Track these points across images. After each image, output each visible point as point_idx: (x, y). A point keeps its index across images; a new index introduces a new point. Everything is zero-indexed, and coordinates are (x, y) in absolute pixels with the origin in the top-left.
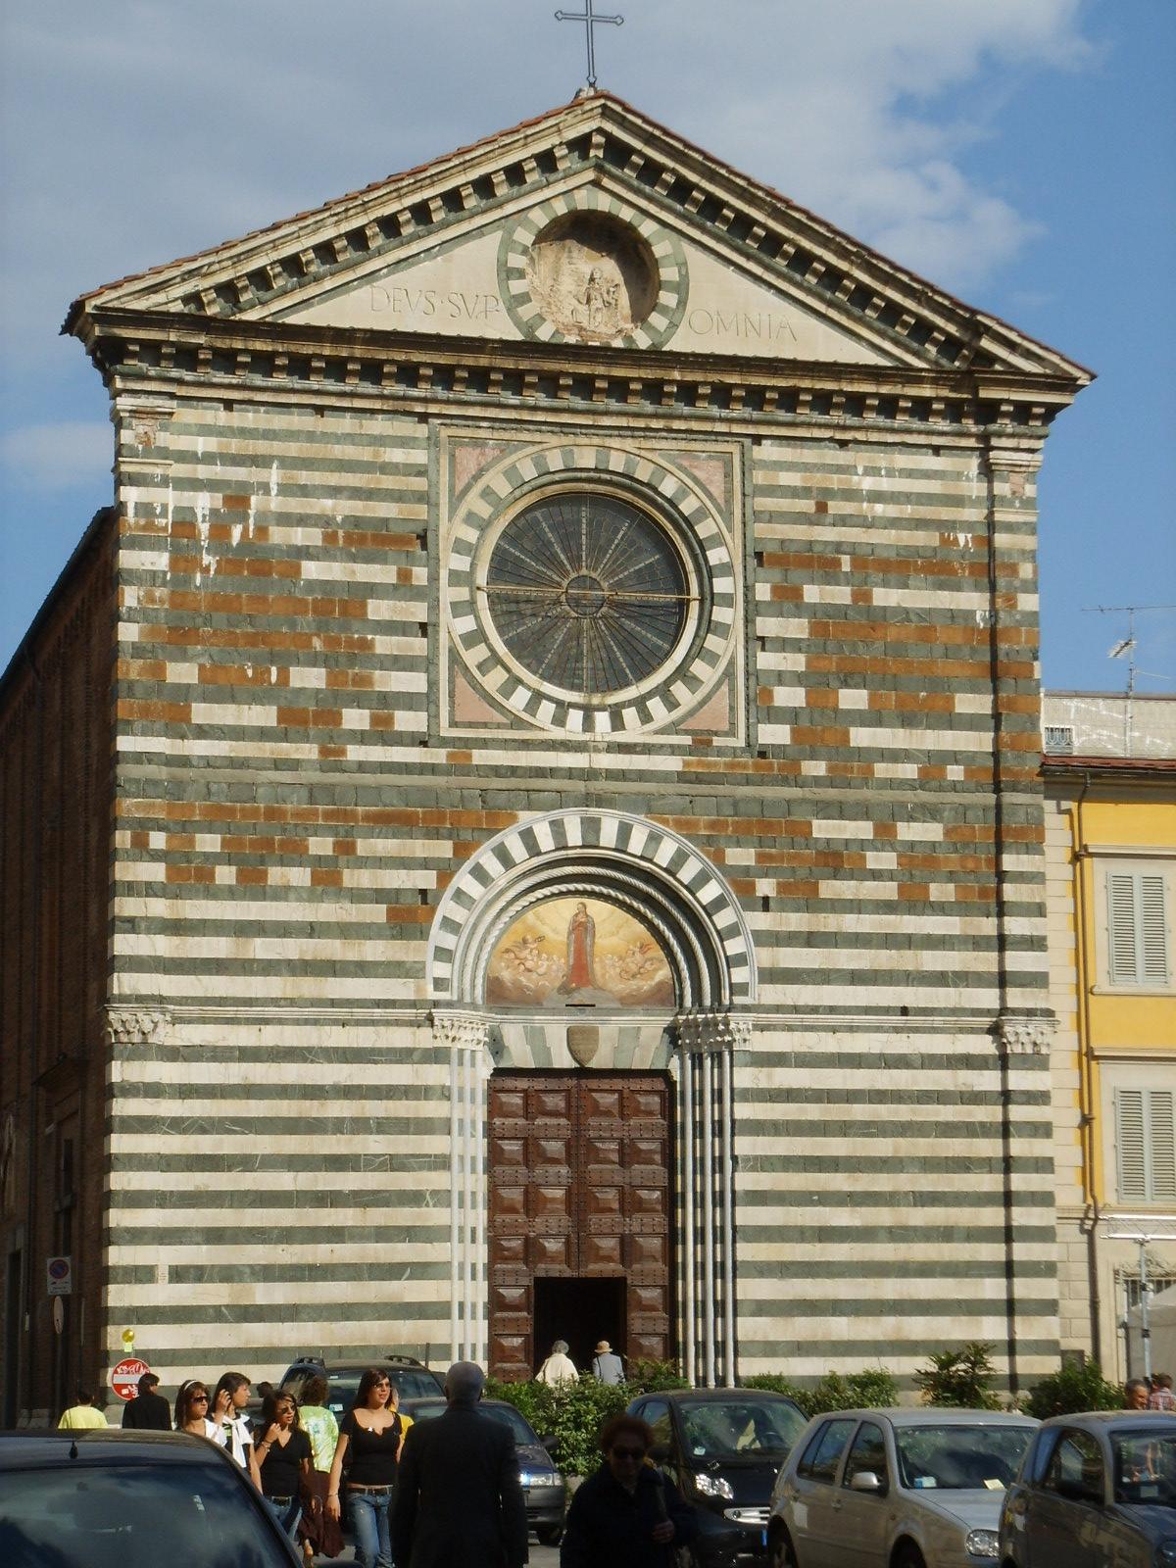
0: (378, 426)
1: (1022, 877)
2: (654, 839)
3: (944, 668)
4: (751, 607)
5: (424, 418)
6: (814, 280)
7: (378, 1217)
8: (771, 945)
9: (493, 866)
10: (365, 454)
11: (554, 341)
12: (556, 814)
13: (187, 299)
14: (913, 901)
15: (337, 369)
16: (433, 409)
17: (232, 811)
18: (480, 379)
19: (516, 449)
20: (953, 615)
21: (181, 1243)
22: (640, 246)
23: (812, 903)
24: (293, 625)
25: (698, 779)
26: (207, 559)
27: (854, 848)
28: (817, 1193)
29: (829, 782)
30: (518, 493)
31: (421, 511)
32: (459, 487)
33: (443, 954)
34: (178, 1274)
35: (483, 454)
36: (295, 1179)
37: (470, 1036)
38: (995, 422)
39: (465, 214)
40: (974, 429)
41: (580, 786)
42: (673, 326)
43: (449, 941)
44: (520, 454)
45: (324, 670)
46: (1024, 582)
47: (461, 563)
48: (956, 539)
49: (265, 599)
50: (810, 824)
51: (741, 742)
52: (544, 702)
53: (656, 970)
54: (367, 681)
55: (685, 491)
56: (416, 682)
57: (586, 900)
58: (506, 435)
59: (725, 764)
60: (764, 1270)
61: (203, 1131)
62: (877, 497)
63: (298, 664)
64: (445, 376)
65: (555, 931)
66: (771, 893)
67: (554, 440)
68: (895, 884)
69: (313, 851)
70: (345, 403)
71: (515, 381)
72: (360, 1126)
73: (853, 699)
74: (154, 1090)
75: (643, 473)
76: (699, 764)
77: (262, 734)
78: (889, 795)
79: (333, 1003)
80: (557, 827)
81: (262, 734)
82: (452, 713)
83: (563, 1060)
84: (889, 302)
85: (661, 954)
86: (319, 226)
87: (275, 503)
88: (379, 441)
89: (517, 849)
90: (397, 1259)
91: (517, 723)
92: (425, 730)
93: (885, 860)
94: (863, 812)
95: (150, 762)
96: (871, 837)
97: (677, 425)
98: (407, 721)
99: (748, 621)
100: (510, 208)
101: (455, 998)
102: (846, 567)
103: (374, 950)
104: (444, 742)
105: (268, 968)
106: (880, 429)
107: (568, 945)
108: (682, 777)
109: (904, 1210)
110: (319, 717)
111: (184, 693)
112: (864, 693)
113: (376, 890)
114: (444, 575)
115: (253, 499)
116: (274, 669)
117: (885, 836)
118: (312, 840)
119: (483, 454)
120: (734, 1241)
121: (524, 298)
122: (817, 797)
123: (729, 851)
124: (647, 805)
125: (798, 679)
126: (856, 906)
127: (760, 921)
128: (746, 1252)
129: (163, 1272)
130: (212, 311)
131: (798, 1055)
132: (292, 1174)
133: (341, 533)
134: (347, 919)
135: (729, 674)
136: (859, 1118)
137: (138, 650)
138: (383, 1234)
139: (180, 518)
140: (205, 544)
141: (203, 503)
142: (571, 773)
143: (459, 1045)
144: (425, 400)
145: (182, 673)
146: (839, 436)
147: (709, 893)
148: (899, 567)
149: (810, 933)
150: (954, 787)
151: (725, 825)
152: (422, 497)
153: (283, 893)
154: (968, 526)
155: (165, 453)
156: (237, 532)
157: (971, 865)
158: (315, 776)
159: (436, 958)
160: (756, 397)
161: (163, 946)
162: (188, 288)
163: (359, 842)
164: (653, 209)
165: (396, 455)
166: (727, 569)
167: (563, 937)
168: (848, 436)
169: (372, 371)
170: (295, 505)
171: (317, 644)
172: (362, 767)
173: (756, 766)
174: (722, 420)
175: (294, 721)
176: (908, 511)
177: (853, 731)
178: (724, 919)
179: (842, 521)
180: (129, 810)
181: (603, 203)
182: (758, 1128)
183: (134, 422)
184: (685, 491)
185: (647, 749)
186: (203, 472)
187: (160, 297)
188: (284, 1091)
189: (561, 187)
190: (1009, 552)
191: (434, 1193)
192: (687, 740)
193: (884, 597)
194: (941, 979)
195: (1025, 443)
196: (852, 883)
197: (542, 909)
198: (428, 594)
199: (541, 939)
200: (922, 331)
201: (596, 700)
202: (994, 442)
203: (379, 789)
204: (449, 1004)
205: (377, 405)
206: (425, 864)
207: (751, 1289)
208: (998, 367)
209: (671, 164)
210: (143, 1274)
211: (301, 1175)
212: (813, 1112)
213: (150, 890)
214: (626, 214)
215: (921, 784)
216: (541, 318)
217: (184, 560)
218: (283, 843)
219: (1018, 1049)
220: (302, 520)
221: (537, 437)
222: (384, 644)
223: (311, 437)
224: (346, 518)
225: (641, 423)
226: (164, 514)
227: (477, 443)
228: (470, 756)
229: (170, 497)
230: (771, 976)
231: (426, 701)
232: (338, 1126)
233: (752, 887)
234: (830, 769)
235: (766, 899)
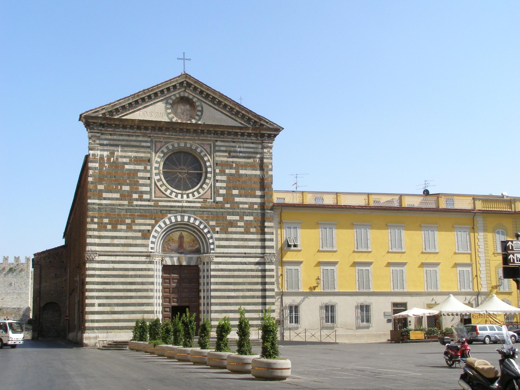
0: (140, 139)
2: (195, 219)
3: (254, 186)
4: (215, 174)
5: (150, 137)
6: (228, 110)
7: (139, 294)
8: (219, 241)
10: (138, 144)
11: (176, 122)
13: (102, 114)
14: (247, 232)
15: (132, 127)
17: (111, 214)
18: (160, 129)
19: (168, 143)
20: (256, 175)
21: (100, 299)
22: (194, 103)
23: (226, 232)
24: (123, 178)
25: (204, 208)
26: (106, 165)
27: (235, 222)
28: (227, 289)
29: (230, 208)
30: (168, 152)
31: (149, 155)
33: (153, 243)
34: (100, 305)
35: (162, 144)
36: (123, 287)
37: (158, 259)
38: (264, 137)
43: (154, 240)
44: (169, 144)
46: (270, 169)
47: (157, 165)
48: (256, 160)
49: (117, 172)
50: (227, 217)
51: (212, 201)
52: (173, 193)
53: (196, 246)
55: (202, 151)
56: (147, 189)
57: (182, 232)
58: (166, 140)
60: (216, 304)
61: (105, 277)
62: (240, 152)
63: (124, 185)
64: (154, 129)
65: (176, 238)
66: (219, 230)
67: (176, 141)
68: (243, 228)
69: (127, 222)
70: (134, 134)
71: (168, 129)
72: (136, 276)
73: (235, 192)
74: (94, 269)
75: (194, 148)
76: (204, 205)
77: (117, 199)
79: (131, 252)
81: (117, 199)
84: (243, 114)
85: (197, 242)
86: (128, 100)
87: (120, 154)
88: (141, 141)
90: (143, 302)
91: (168, 197)
92: (149, 198)
94: (237, 214)
95: (94, 205)
98: (146, 196)
99: (214, 177)
100: (168, 96)
101: (155, 251)
102: (234, 166)
103: (139, 242)
104: (153, 201)
105: (118, 245)
106: (241, 139)
107: (178, 241)
108: (201, 207)
109: (245, 292)
110: (128, 196)
111: (101, 191)
112: (238, 191)
113: (139, 230)
114: (153, 168)
115: (115, 153)
116: (119, 186)
117: (241, 219)
118: (126, 220)
119: (162, 144)
120: (211, 299)
123: (210, 222)
124: (194, 213)
125: (224, 188)
126: (236, 233)
127: (216, 236)
128: (213, 301)
129: (96, 305)
130: (108, 116)
132: (122, 286)
133: (133, 159)
134: (133, 235)
135: (211, 187)
136: (236, 274)
137: (92, 183)
139: (101, 157)
140: (106, 162)
141: (106, 154)
142: (179, 207)
143: (155, 261)
144: (150, 134)
145: (101, 187)
146: (233, 140)
149: (227, 238)
150: (256, 209)
153: (121, 230)
156: (112, 159)
158: (127, 207)
159: (151, 243)
160: (216, 133)
161: (97, 241)
162: (103, 111)
163: (136, 220)
164: (196, 96)
165: (144, 144)
166: (210, 166)
167: (177, 239)
168: (235, 140)
169: (139, 128)
170: (124, 154)
171: (128, 181)
172: (136, 205)
175: (123, 197)
177: (235, 198)
178: (209, 236)
180: (90, 214)
181: (186, 95)
182: (215, 276)
183: (92, 138)
184: (202, 151)
185: (194, 202)
187: (97, 114)
188: (121, 269)
189: (178, 92)
190: (267, 163)
191: (151, 289)
192: (202, 200)
193: (242, 172)
194: (252, 247)
196: (235, 228)
197: (172, 234)
198: (150, 171)
199: (173, 239)
200: (249, 119)
201: (184, 192)
203: (140, 209)
205: (140, 134)
206: (149, 225)
207: (214, 308)
208: (265, 127)
209: (199, 87)
210: (93, 305)
211: (124, 286)
212: (227, 273)
213: (94, 230)
214: (191, 97)
217: (102, 165)
218: (121, 221)
220: (125, 157)
222: (141, 181)
223: (127, 141)
226: (97, 156)
227: (161, 142)
229: (99, 153)
230: (219, 247)
231: (150, 193)
232: (131, 276)
233: (215, 229)
235: (218, 231)
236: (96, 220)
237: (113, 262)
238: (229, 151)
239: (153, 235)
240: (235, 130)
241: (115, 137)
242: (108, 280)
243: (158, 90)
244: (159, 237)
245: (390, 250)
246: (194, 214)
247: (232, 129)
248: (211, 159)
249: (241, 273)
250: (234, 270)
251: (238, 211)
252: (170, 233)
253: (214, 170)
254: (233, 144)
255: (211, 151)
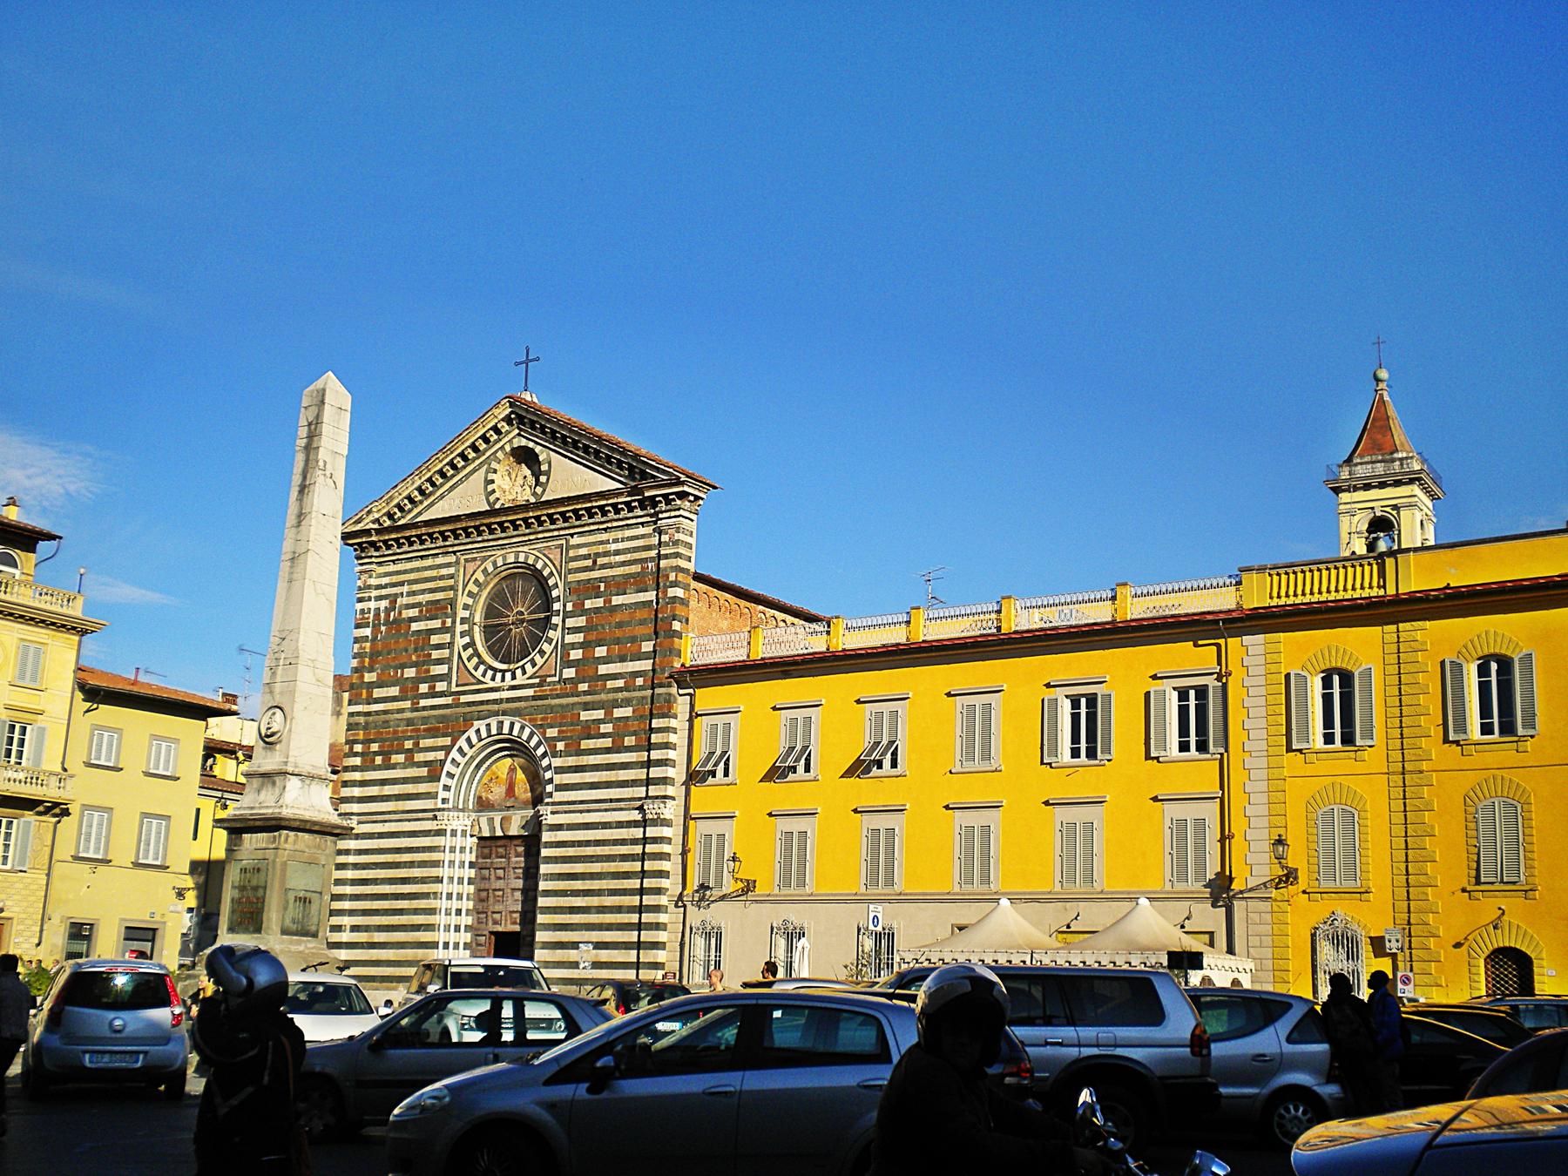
0: (440, 560)
1: (660, 730)
2: (522, 728)
9: (466, 748)
12: (487, 721)
14: (618, 748)
16: (456, 549)
24: (406, 651)
31: (451, 594)
32: (466, 581)
33: (447, 788)
34: (355, 929)
39: (470, 462)
40: (652, 511)
41: (496, 707)
42: (544, 490)
43: (449, 782)
45: (414, 669)
46: (671, 582)
47: (466, 614)
50: (579, 714)
54: (428, 671)
56: (443, 669)
58: (483, 554)
59: (550, 690)
61: (364, 869)
62: (617, 553)
65: (503, 774)
66: (563, 749)
67: (499, 553)
72: (411, 864)
73: (601, 651)
76: (540, 691)
77: (394, 699)
78: (611, 696)
80: (488, 725)
81: (394, 699)
82: (457, 681)
83: (499, 833)
88: (440, 566)
89: (474, 740)
90: (420, 923)
93: (606, 728)
96: (603, 717)
97: (540, 536)
98: (441, 686)
99: (564, 621)
100: (488, 454)
101: (450, 806)
102: (602, 589)
103: (423, 788)
108: (534, 698)
109: (603, 898)
111: (371, 686)
112: (605, 648)
115: (398, 600)
116: (399, 671)
121: (494, 491)
122: (583, 701)
127: (557, 762)
131: (568, 824)
133: (424, 609)
135: (556, 647)
138: (416, 911)
141: (384, 604)
145: (369, 677)
147: (540, 751)
148: (620, 585)
150: (641, 688)
151: (548, 718)
152: (451, 588)
153: (394, 767)
154: (652, 559)
155: (369, 587)
156: (392, 614)
157: (642, 726)
158: (408, 715)
159: (444, 790)
162: (371, 518)
163: (421, 741)
165: (444, 572)
168: (604, 526)
170: (412, 600)
172: (424, 708)
173: (561, 689)
174: (555, 530)
176: (628, 557)
178: (545, 763)
179: (603, 567)
181: (524, 442)
184: (546, 565)
186: (384, 592)
189: (506, 439)
191: (435, 893)
192: (537, 680)
193: (616, 600)
195: (673, 514)
202: (660, 516)
204: (449, 810)
213: (355, 769)
214: (531, 445)
215: (625, 689)
216: (498, 499)
219: (651, 817)
220: (413, 606)
221: (493, 553)
222: (435, 654)
223: (418, 570)
224: (427, 602)
225: (526, 538)
227: (474, 559)
228: (459, 699)
229: (372, 605)
230: (560, 788)
234: (589, 687)
236: (358, 748)
237: (381, 835)
238: (595, 554)
239: (448, 772)
240: (596, 501)
241: (399, 567)
242: (368, 874)
243: (463, 447)
244: (463, 774)
245: (958, 769)
246: (520, 716)
247: (591, 501)
248: (561, 580)
249: (599, 850)
250: (587, 843)
251: (603, 696)
252: (492, 764)
253: (565, 606)
254: (604, 537)
255: (562, 561)
